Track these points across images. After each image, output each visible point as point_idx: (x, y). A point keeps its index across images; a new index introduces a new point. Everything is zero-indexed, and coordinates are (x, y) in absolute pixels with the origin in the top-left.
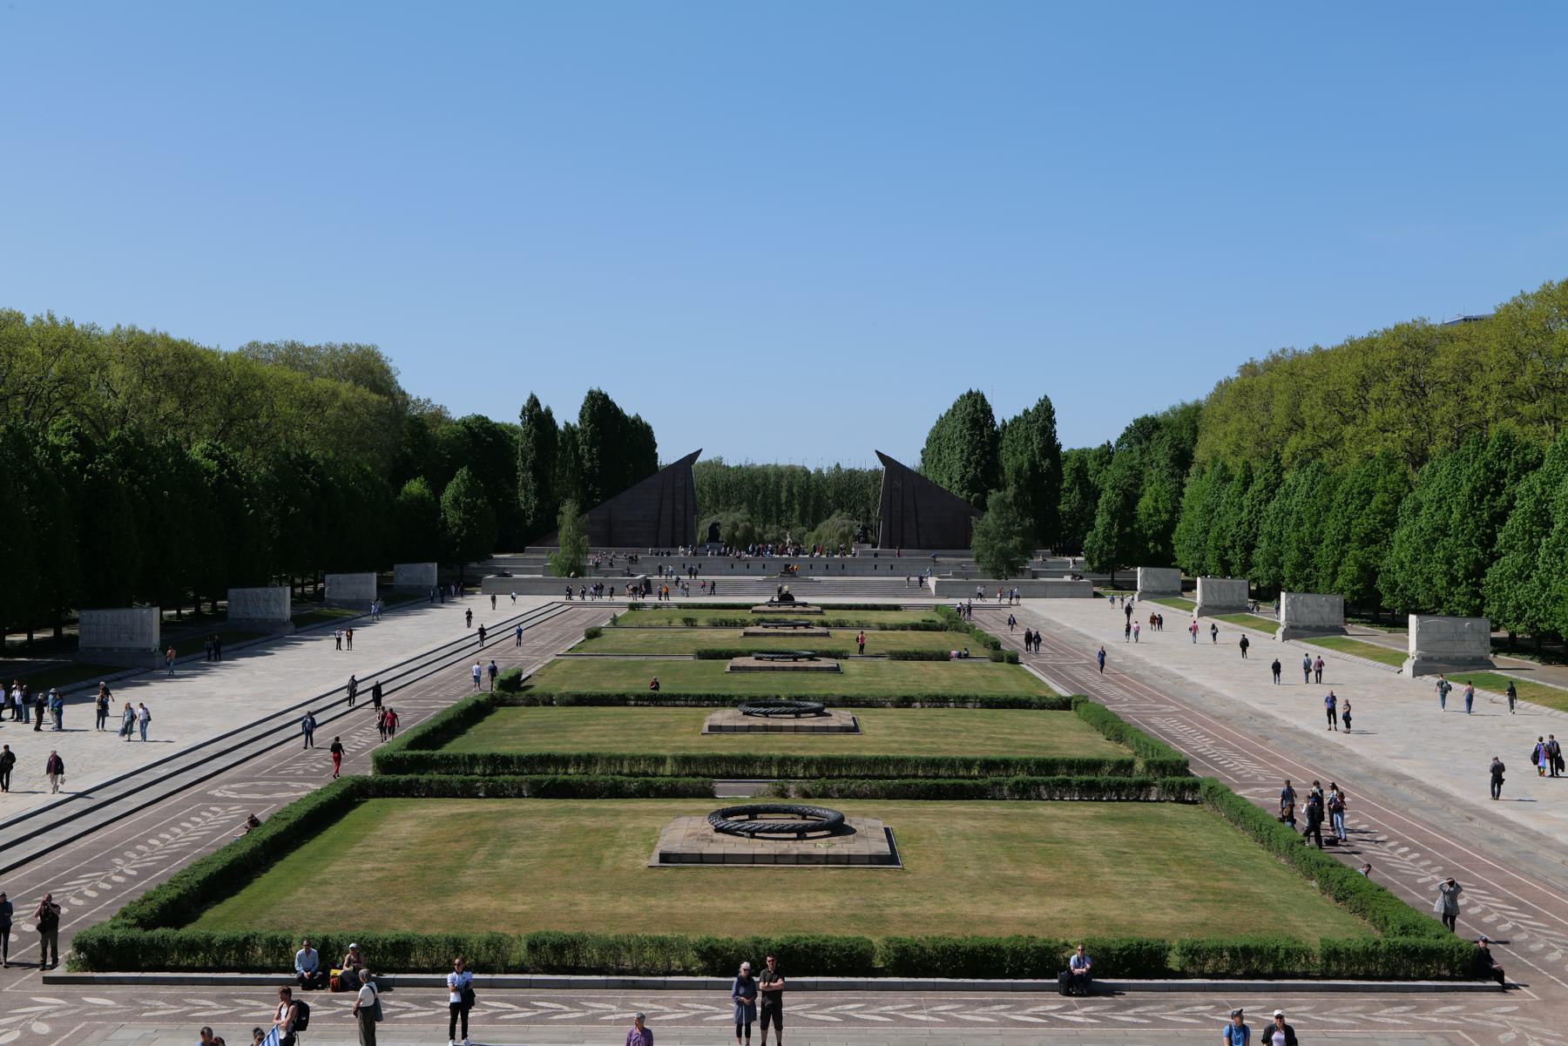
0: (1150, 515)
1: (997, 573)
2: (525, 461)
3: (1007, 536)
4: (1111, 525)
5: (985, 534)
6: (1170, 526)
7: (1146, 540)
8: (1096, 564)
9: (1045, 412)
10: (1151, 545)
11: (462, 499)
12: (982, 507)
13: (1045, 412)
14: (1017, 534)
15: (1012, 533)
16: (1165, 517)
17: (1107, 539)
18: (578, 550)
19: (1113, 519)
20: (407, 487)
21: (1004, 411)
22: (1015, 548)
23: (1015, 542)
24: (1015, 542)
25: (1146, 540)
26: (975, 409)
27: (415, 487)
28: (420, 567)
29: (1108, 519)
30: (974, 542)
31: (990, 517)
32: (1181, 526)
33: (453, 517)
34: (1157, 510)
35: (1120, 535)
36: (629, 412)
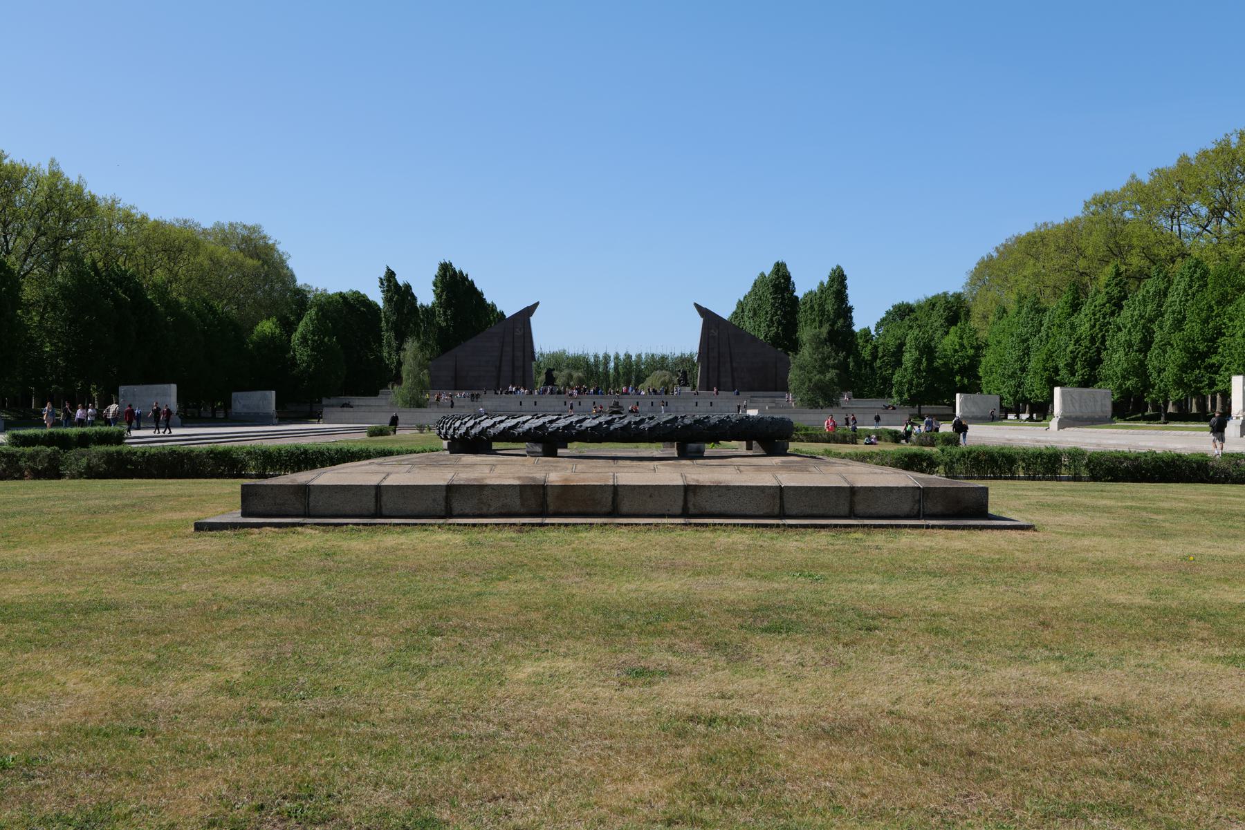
0: (956, 351)
1: (813, 405)
2: (387, 322)
3: (824, 368)
4: (918, 361)
5: (802, 368)
6: (974, 363)
7: (952, 373)
8: (906, 396)
9: (839, 280)
10: (958, 378)
11: (309, 336)
12: (795, 346)
13: (839, 280)
14: (834, 367)
15: (828, 367)
16: (971, 352)
17: (917, 371)
18: (422, 386)
19: (921, 355)
20: (259, 328)
21: (806, 283)
22: (832, 380)
23: (831, 374)
24: (831, 374)
25: (952, 373)
26: (780, 281)
27: (267, 326)
28: (258, 395)
29: (916, 354)
30: (790, 376)
31: (806, 353)
32: (988, 359)
33: (302, 354)
34: (962, 345)
35: (931, 370)
36: (489, 301)
